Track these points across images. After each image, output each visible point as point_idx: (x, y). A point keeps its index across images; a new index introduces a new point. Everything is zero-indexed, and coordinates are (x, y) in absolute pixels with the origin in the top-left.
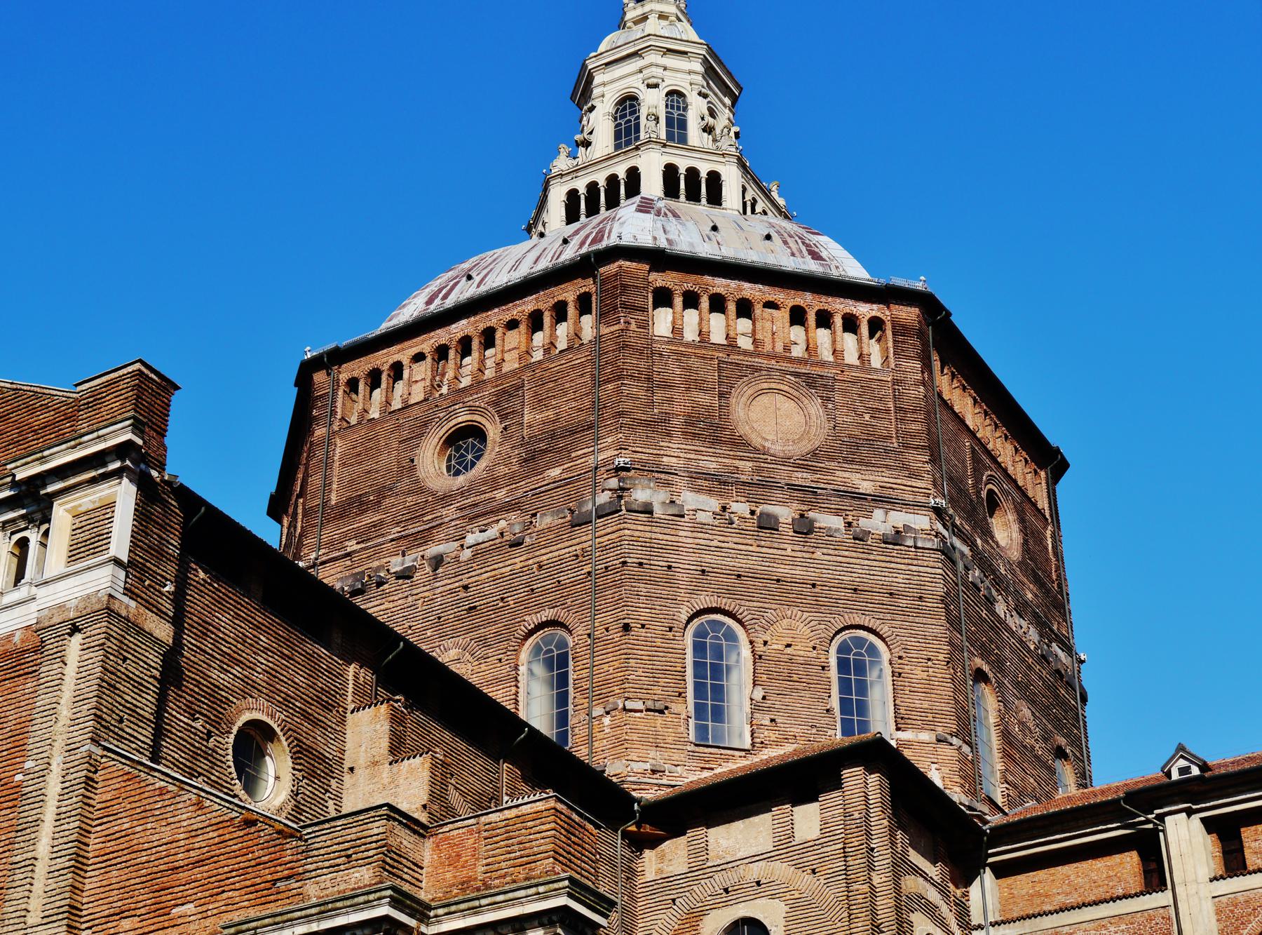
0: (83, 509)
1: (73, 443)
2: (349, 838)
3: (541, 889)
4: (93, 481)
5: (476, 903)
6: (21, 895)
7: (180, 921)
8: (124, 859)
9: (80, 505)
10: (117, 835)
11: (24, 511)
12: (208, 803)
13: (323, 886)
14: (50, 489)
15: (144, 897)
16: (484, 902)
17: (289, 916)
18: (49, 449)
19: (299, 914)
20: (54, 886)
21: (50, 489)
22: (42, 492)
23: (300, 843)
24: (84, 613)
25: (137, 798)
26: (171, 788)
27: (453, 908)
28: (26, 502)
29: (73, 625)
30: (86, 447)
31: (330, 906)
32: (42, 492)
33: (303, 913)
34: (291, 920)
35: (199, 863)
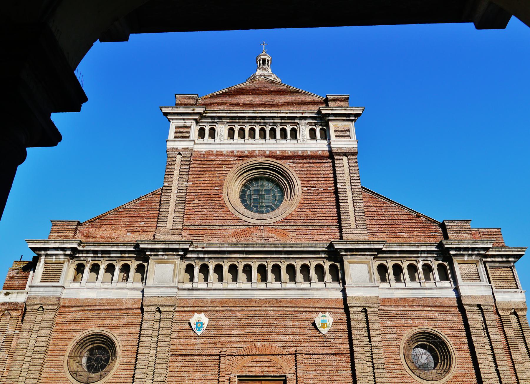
0: (338, 126)
1: (343, 109)
2: (460, 226)
3: (519, 249)
4: (344, 120)
5: (501, 249)
6: (347, 220)
7: (401, 237)
8: (377, 217)
9: (338, 125)
10: (371, 211)
11: (316, 121)
12: (402, 209)
13: (455, 236)
14: (330, 118)
15: (387, 229)
16: (503, 249)
17: (463, 242)
18: (335, 108)
19: (466, 242)
20: (359, 219)
21: (330, 118)
22: (327, 118)
23: (436, 225)
24: (350, 152)
25: (376, 203)
26: (388, 202)
27: (494, 249)
28: (318, 119)
29: (345, 154)
30: (347, 111)
31: (476, 242)
32: (327, 118)
33: (468, 242)
34: (463, 243)
35: (403, 223)
